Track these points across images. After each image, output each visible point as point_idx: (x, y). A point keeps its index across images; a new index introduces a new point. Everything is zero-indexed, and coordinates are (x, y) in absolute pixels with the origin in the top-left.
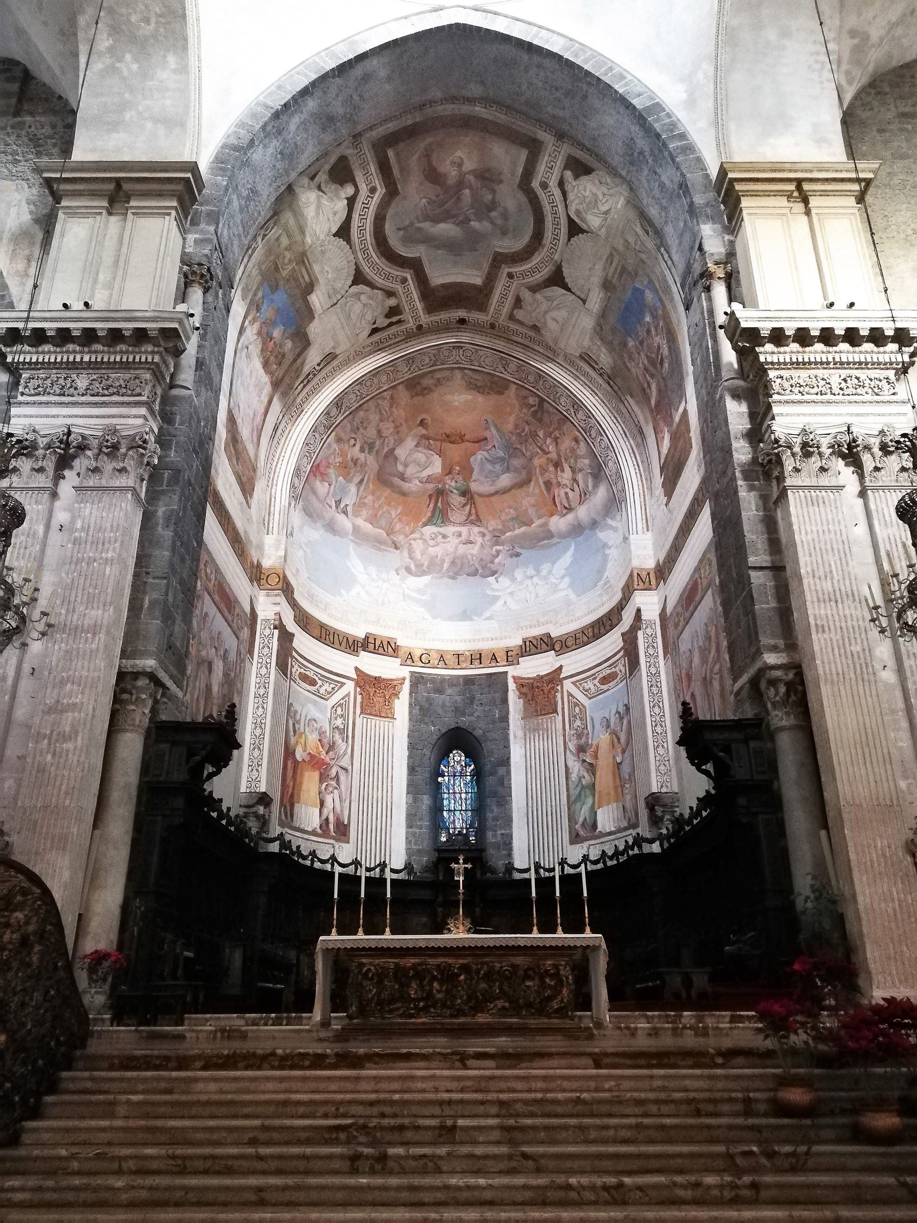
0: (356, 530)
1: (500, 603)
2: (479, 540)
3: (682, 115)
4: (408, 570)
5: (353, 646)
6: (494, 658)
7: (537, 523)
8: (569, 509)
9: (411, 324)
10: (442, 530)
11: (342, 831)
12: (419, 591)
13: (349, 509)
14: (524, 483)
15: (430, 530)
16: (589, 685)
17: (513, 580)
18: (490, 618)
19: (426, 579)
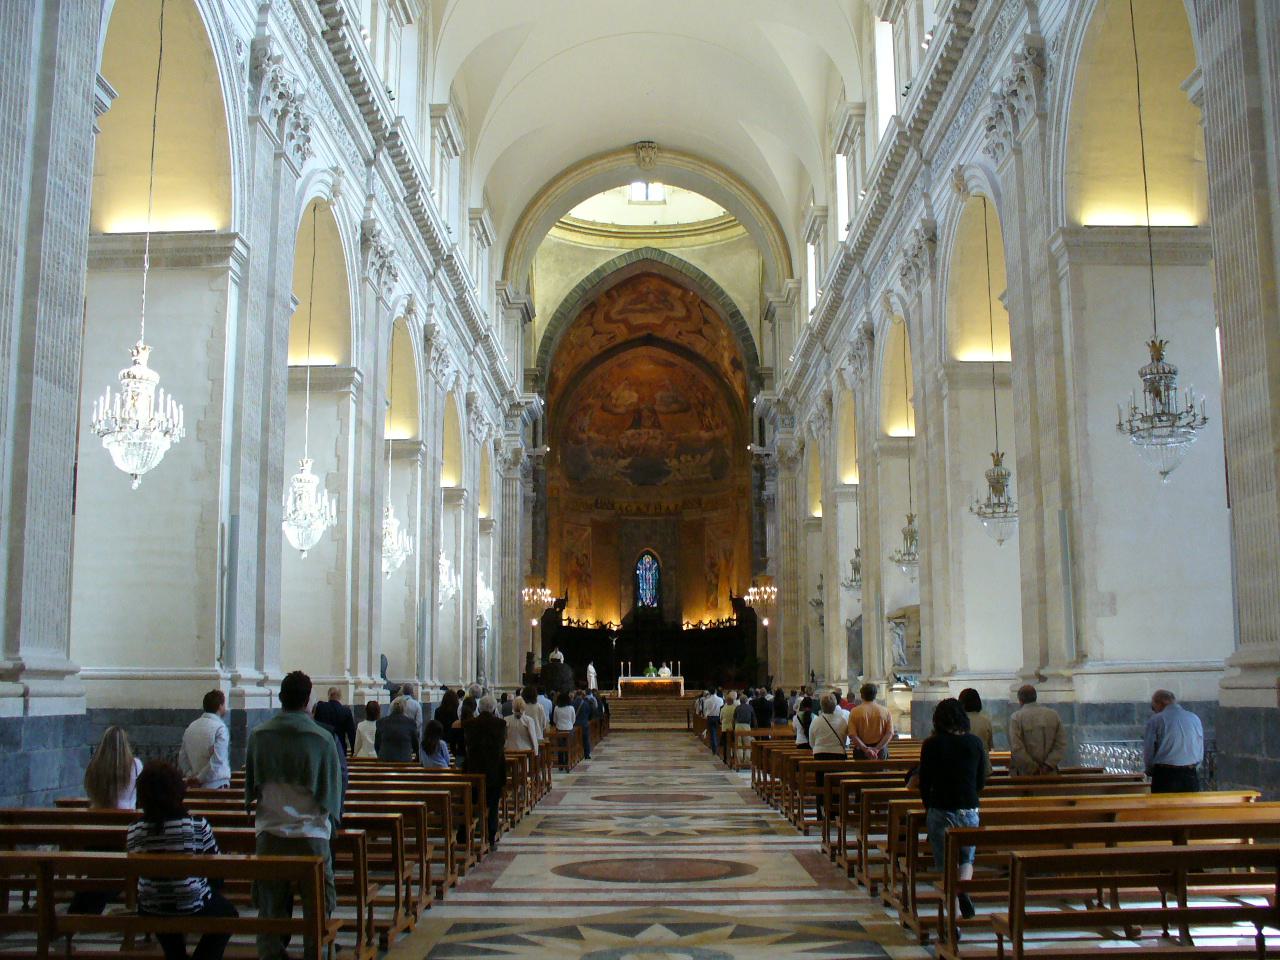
1: (672, 475)
2: (660, 437)
3: (746, 319)
10: (638, 431)
12: (626, 468)
13: (586, 429)
15: (630, 433)
17: (680, 461)
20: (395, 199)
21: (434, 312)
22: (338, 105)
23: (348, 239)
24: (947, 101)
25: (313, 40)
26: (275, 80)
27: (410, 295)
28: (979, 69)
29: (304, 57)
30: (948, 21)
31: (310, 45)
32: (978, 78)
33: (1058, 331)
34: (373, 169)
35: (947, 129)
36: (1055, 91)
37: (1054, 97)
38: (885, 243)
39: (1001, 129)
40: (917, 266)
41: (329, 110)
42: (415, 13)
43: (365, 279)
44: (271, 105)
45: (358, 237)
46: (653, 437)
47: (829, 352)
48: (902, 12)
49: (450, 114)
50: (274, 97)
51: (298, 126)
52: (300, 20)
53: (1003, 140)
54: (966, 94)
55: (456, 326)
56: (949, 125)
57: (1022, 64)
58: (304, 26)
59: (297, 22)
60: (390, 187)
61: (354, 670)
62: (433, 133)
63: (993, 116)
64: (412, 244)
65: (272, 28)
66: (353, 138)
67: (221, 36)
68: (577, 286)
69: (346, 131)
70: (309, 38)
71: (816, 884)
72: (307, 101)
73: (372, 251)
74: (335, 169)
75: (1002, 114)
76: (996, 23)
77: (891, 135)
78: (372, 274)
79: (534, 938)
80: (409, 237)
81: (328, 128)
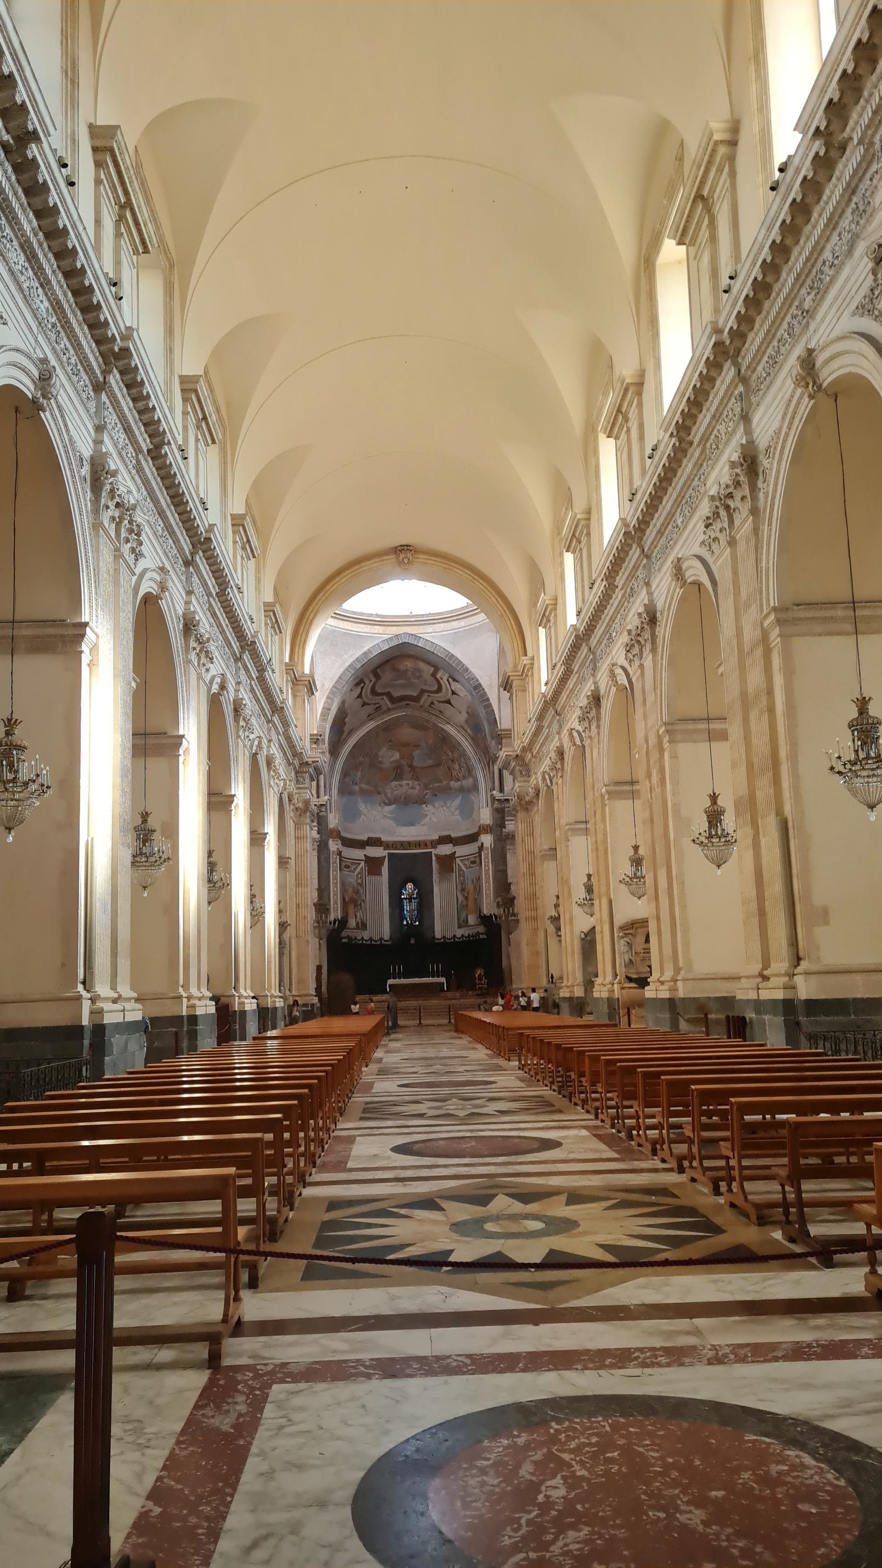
0: (361, 789)
1: (428, 817)
3: (486, 690)
4: (386, 804)
5: (361, 844)
6: (426, 845)
7: (445, 782)
8: (458, 780)
9: (384, 708)
11: (363, 926)
12: (390, 813)
14: (438, 765)
15: (394, 783)
16: (466, 863)
17: (434, 806)
18: (423, 825)
19: (394, 806)
20: (209, 594)
21: (242, 689)
22: (161, 514)
23: (174, 628)
24: (667, 503)
25: (140, 456)
26: (112, 493)
27: (222, 675)
28: (696, 475)
29: (134, 472)
30: (672, 435)
31: (138, 461)
32: (695, 483)
33: (770, 692)
34: (191, 569)
35: (666, 528)
36: (767, 492)
37: (766, 498)
38: (609, 626)
39: (717, 525)
40: (638, 642)
41: (154, 518)
42: (218, 435)
43: (189, 662)
44: (110, 513)
45: (181, 626)
46: (413, 788)
47: (559, 715)
48: (625, 429)
49: (248, 522)
50: (112, 504)
51: (131, 531)
52: (129, 439)
53: (718, 535)
54: (683, 497)
55: (257, 700)
56: (668, 524)
57: (738, 471)
58: (132, 445)
59: (127, 441)
60: (204, 584)
61: (186, 987)
62: (234, 538)
63: (709, 515)
64: (222, 632)
65: (108, 446)
66: (174, 542)
67: (67, 452)
68: (349, 666)
69: (168, 536)
70: (137, 455)
71: (617, 1156)
72: (138, 511)
73: (193, 638)
74: (162, 569)
75: (718, 513)
76: (713, 437)
77: (618, 534)
78: (193, 656)
79: (403, 1211)
80: (219, 626)
81: (155, 534)
